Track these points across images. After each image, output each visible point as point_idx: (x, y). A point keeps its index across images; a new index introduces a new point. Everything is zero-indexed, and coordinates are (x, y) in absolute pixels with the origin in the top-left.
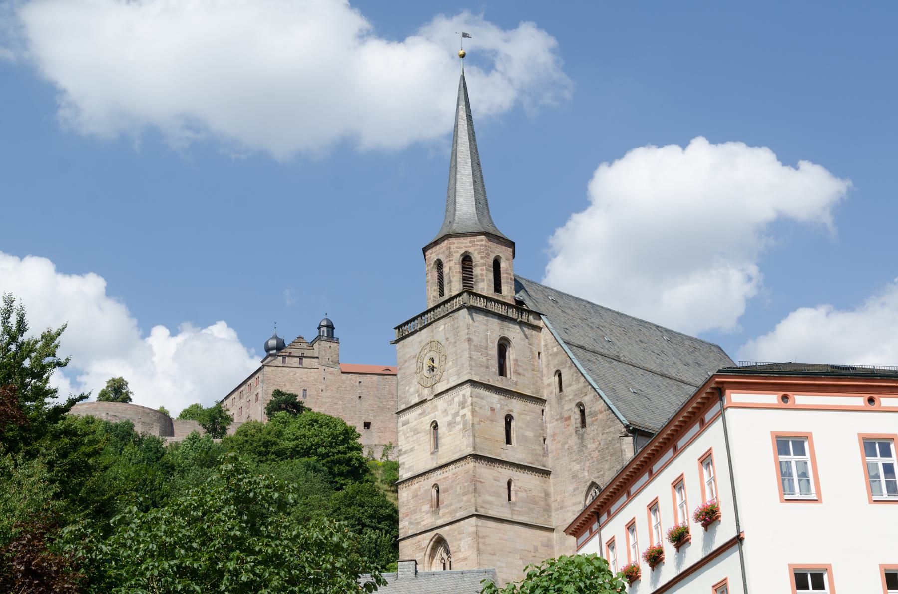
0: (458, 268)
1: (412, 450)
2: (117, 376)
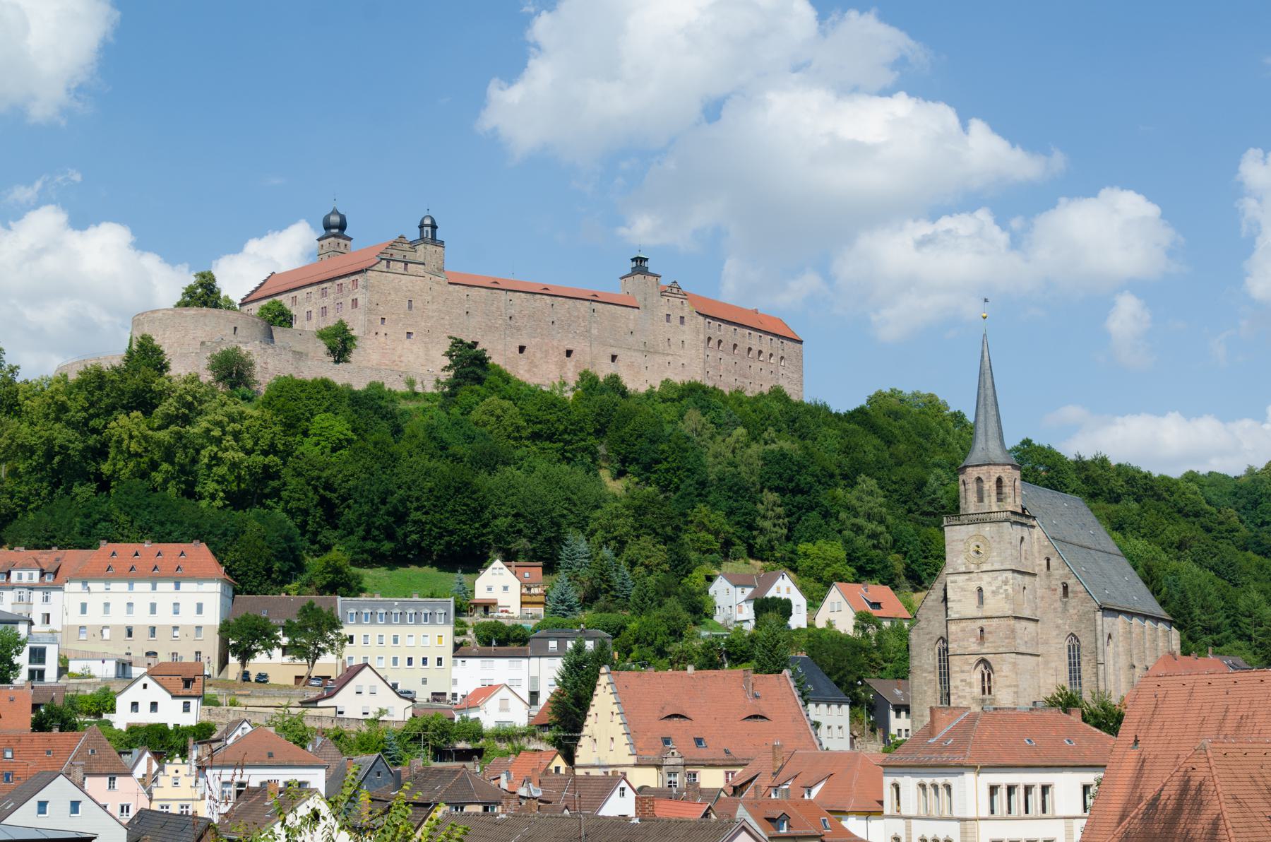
0: (994, 487)
2: (204, 270)
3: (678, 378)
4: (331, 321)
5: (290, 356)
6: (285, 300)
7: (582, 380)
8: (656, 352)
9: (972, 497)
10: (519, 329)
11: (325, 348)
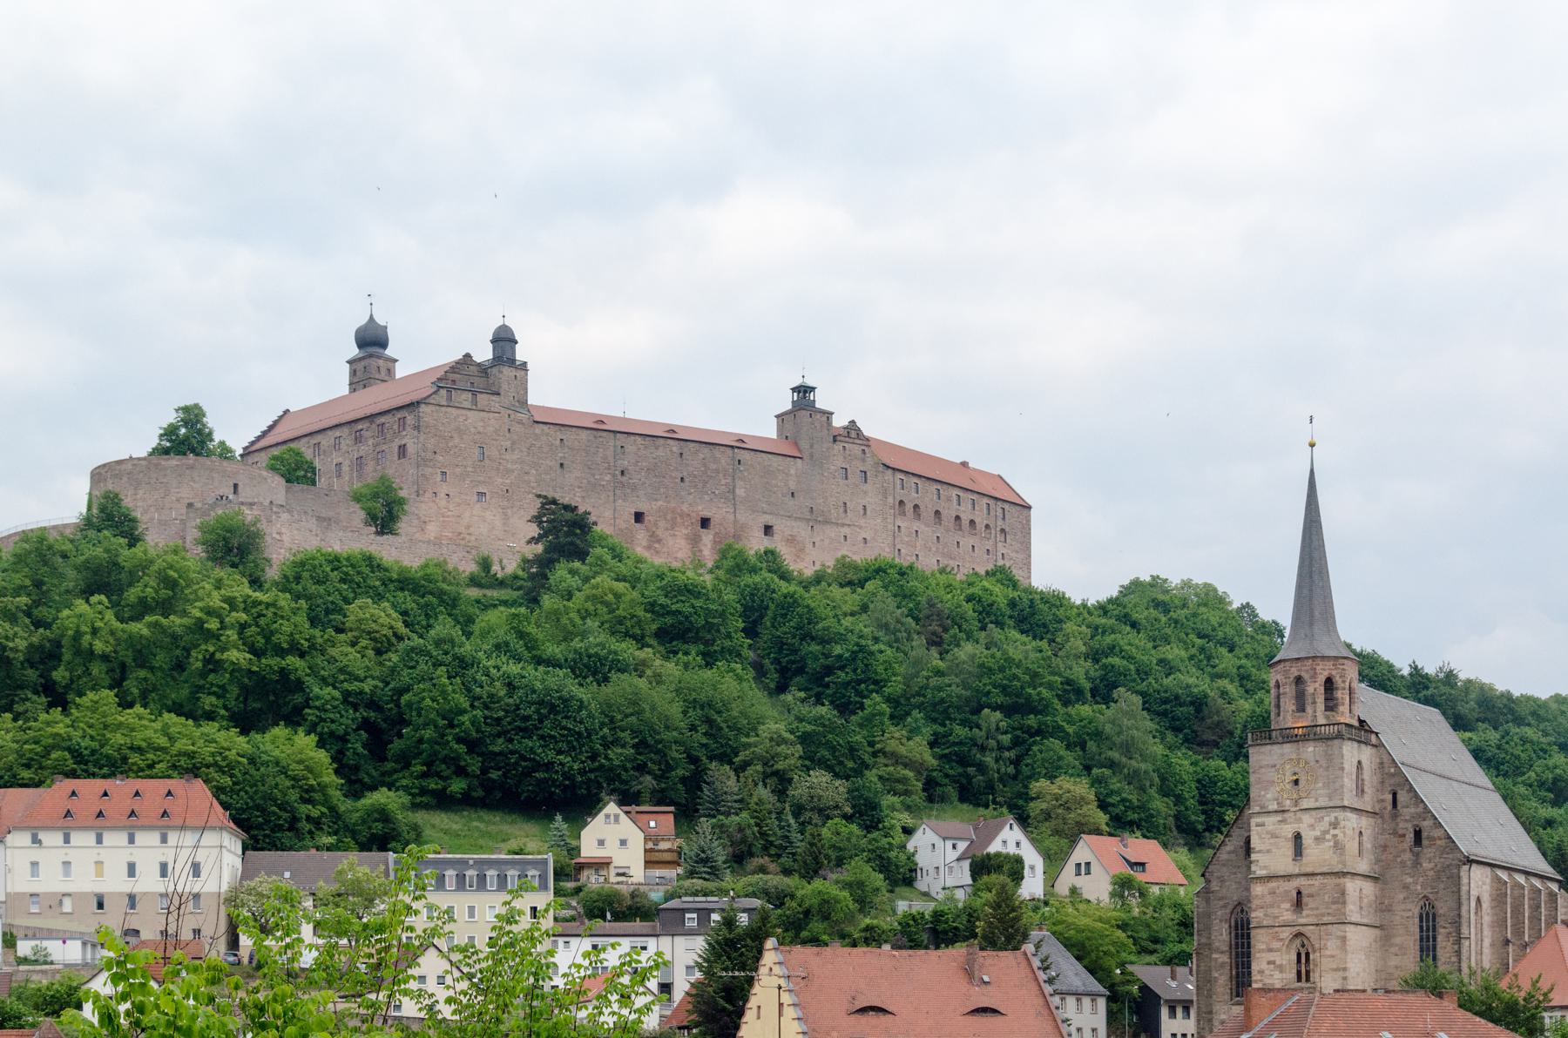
1: (1268, 851)
3: (860, 556)
4: (371, 474)
5: (312, 524)
6: (305, 449)
7: (724, 557)
8: (827, 522)
9: (1289, 705)
10: (634, 488)
11: (362, 515)
